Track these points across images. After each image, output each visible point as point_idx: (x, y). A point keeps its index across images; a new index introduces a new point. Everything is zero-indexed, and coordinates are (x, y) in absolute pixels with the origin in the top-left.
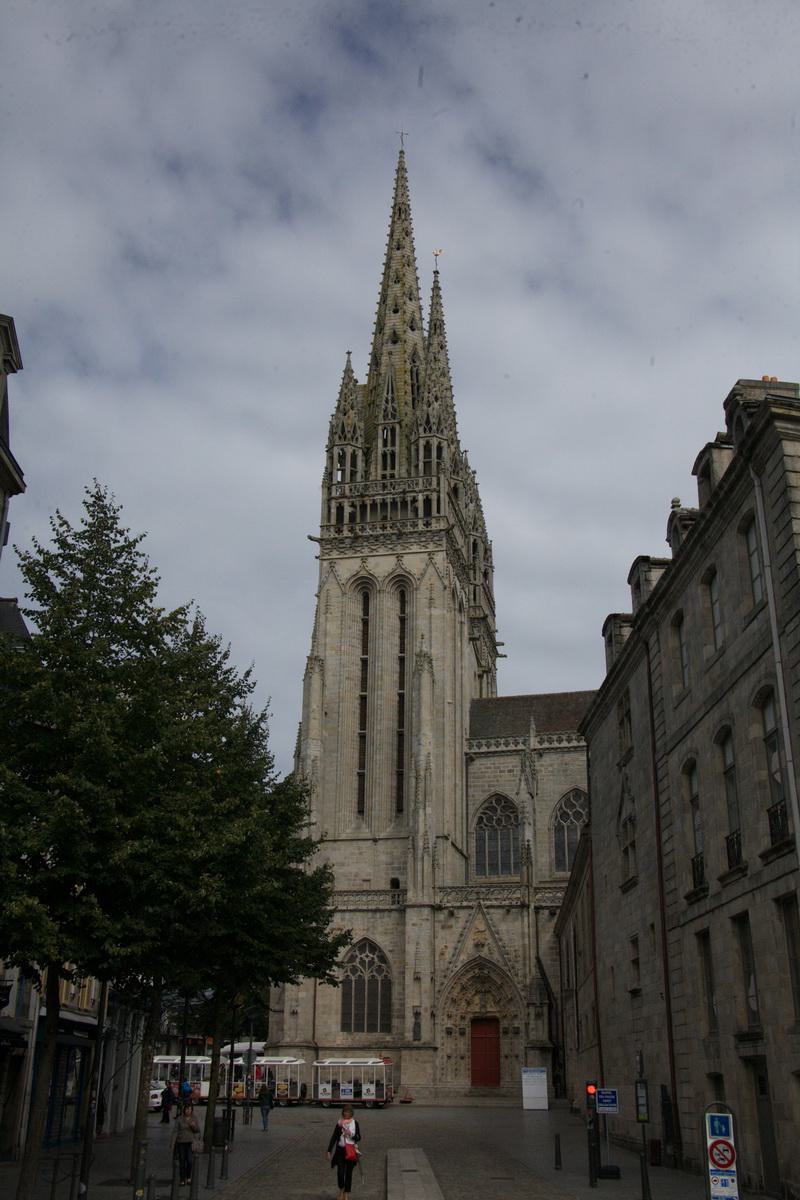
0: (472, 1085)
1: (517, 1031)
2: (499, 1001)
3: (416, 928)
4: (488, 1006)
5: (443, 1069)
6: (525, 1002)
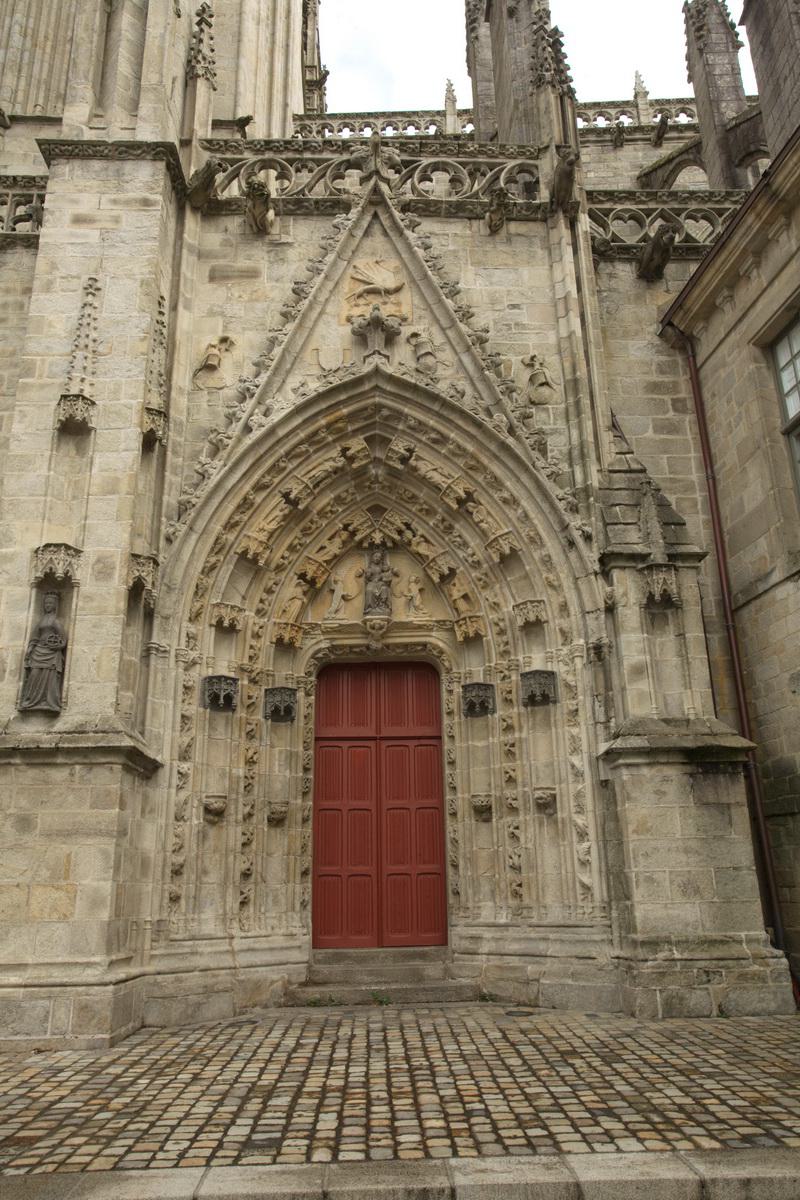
0: (316, 944)
1: (541, 694)
2: (448, 577)
3: (92, 234)
4: (399, 603)
5: (177, 872)
6: (592, 555)
